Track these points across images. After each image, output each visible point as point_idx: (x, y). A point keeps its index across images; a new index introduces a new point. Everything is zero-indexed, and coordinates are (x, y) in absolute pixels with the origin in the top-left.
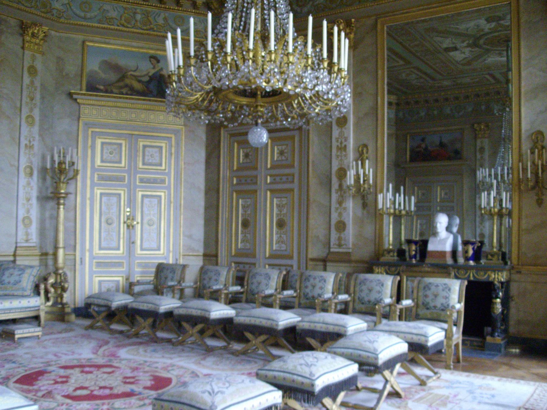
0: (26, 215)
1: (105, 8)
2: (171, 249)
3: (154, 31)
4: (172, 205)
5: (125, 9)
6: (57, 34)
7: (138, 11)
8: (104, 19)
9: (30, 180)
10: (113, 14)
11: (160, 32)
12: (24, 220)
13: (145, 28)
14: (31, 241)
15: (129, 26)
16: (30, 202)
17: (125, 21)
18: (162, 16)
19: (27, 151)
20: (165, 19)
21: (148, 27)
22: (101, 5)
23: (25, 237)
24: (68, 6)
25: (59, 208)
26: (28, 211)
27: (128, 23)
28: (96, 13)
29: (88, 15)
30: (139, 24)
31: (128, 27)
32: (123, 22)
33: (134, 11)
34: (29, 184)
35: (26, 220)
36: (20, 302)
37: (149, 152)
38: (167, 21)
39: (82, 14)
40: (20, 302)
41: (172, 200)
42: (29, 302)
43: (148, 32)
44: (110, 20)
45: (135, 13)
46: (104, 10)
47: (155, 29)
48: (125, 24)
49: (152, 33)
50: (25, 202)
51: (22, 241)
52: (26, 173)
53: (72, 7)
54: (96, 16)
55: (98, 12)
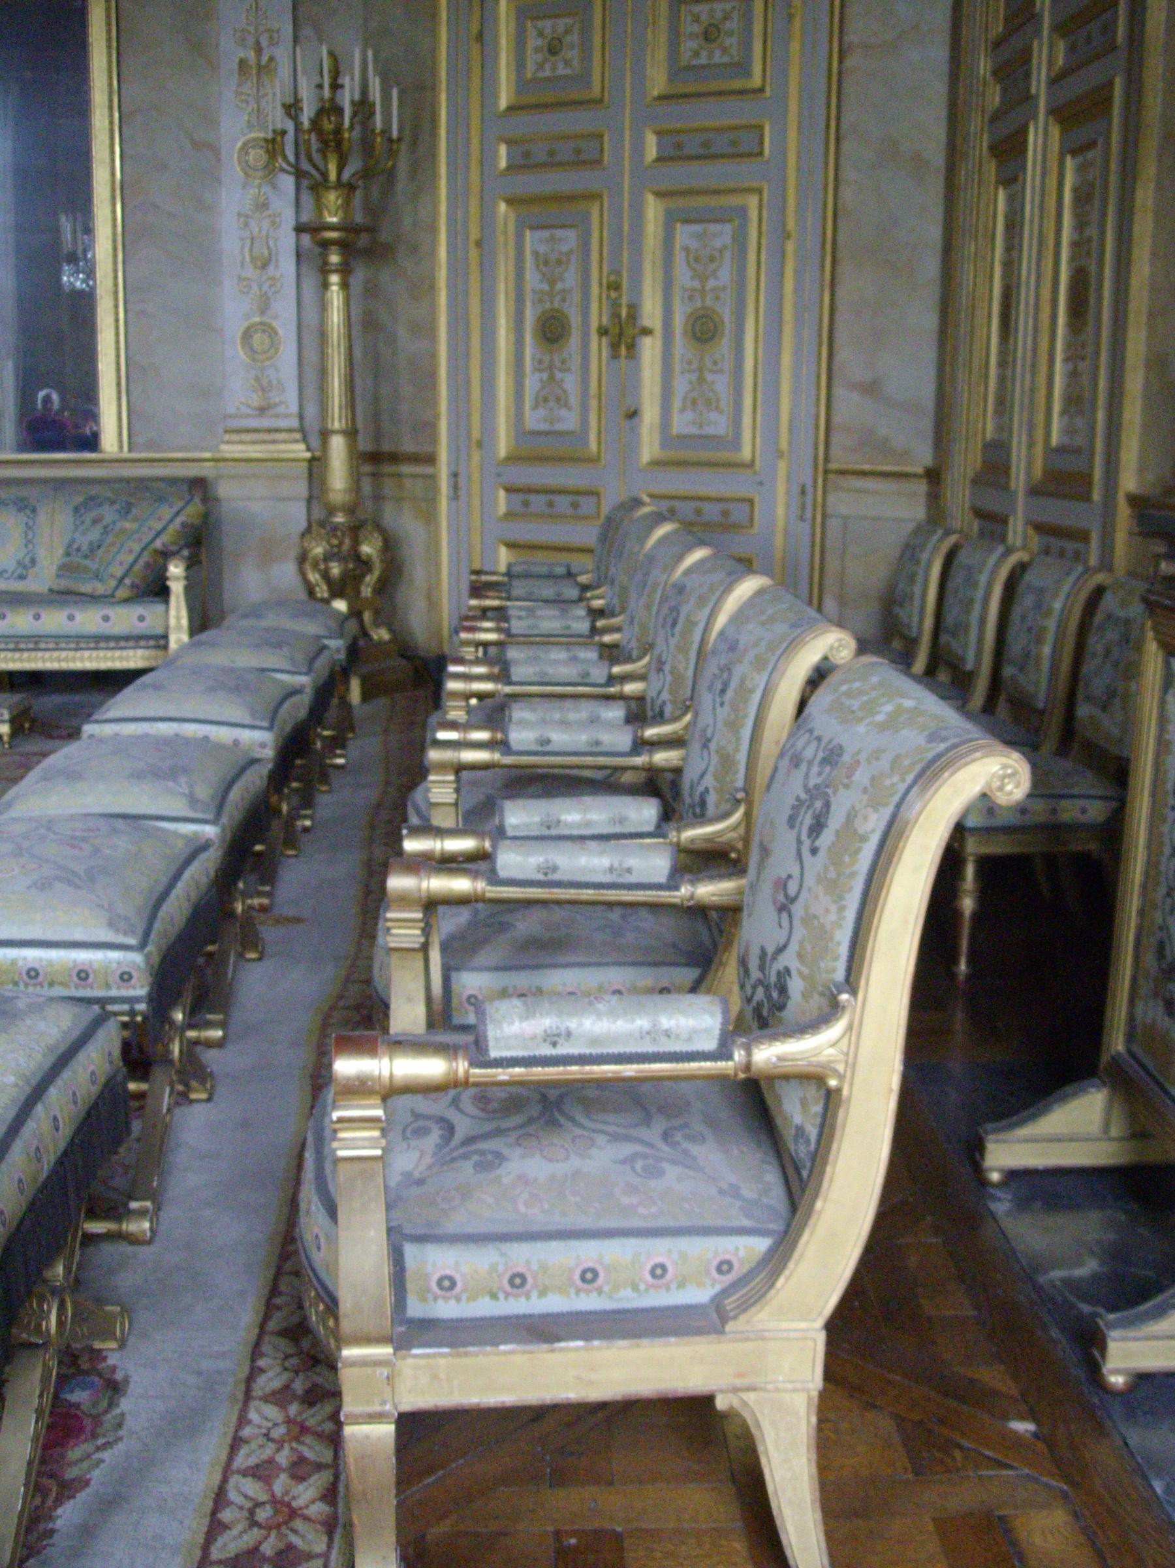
0: (257, 319)
2: (784, 444)
4: (790, 247)
9: (267, 189)
12: (247, 336)
14: (281, 409)
16: (271, 270)
19: (249, 88)
23: (256, 400)
25: (326, 285)
26: (264, 305)
34: (262, 206)
35: (257, 338)
36: (71, 618)
37: (697, 20)
40: (71, 618)
41: (791, 225)
42: (106, 619)
50: (250, 272)
51: (244, 410)
52: (247, 168)
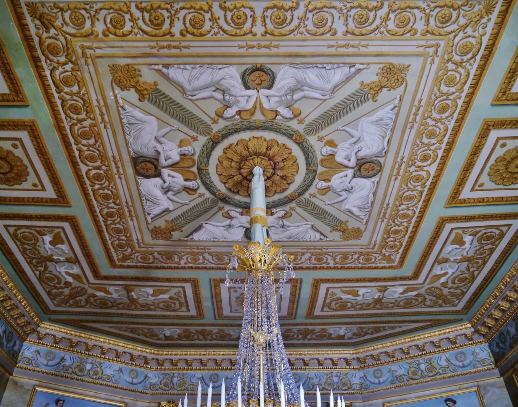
1: (393, 369)
3: (441, 374)
5: (410, 364)
6: (361, 404)
7: (421, 361)
8: (395, 379)
10: (401, 372)
11: (447, 373)
13: (431, 374)
15: (416, 377)
17: (413, 374)
18: (444, 358)
20: (447, 360)
21: (434, 372)
22: (390, 368)
24: (364, 377)
27: (415, 375)
28: (387, 376)
29: (381, 380)
30: (426, 374)
31: (416, 379)
32: (411, 375)
33: (417, 362)
38: (449, 361)
39: (376, 381)
43: (434, 377)
44: (400, 378)
45: (419, 364)
46: (393, 371)
47: (441, 372)
48: (414, 377)
49: (438, 377)
53: (368, 378)
54: (387, 379)
55: (389, 374)
